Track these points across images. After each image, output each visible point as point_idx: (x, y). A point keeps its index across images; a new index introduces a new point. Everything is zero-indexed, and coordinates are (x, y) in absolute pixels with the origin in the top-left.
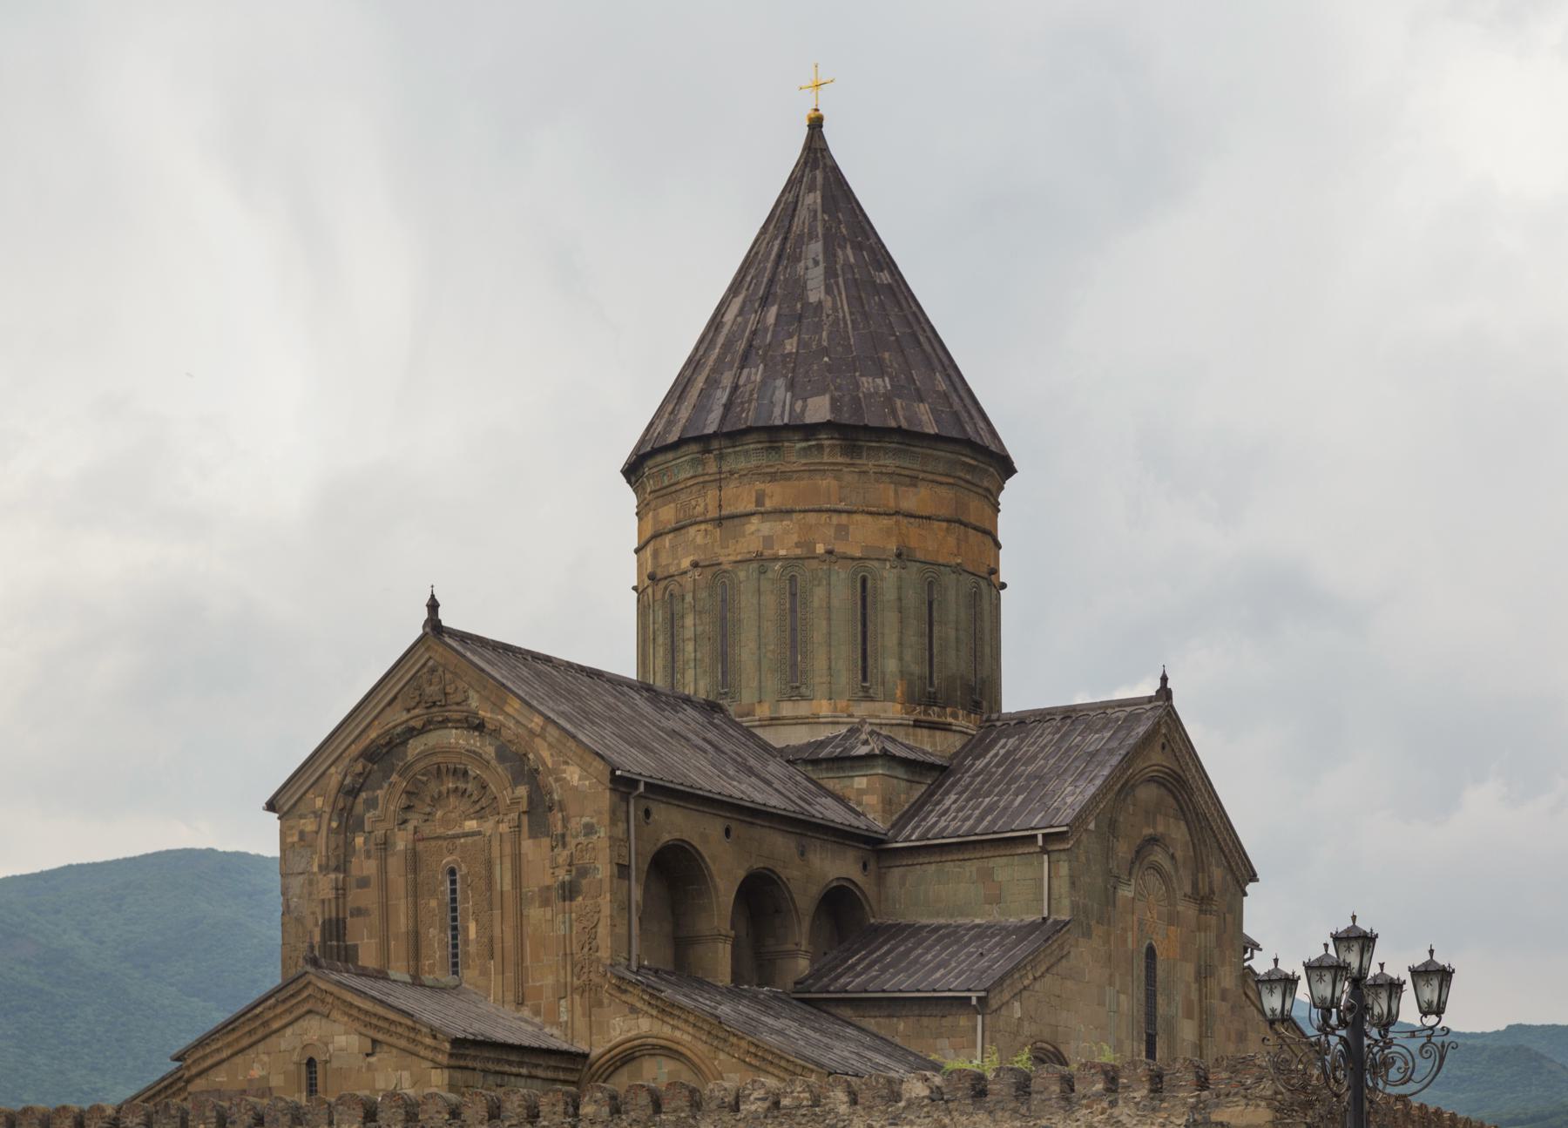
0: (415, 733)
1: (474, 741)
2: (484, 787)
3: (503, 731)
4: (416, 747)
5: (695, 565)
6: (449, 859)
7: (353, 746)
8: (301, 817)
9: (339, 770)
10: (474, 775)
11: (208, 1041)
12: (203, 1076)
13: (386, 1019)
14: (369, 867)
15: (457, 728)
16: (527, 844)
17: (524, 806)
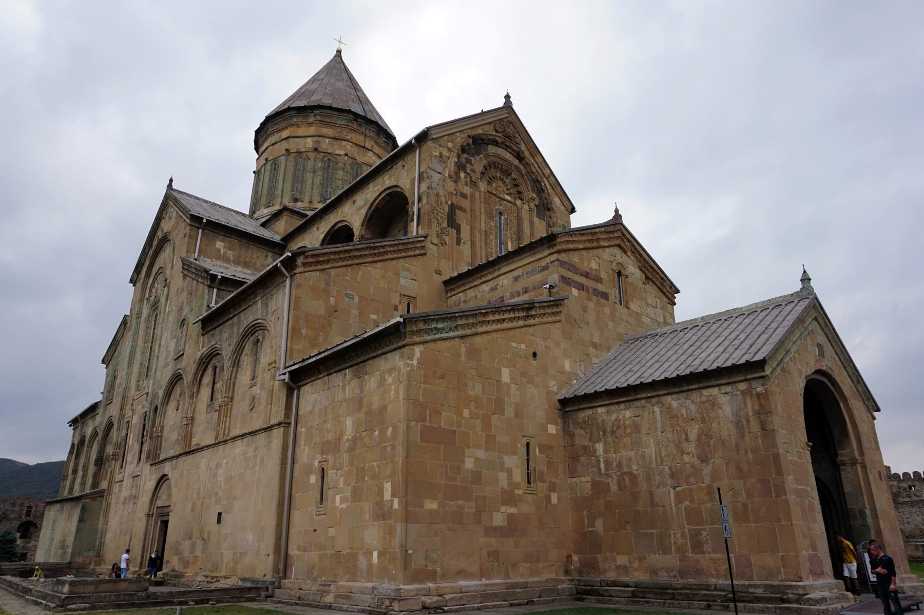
0: (494, 143)
1: (516, 162)
2: (517, 186)
3: (532, 166)
4: (492, 149)
5: (346, 155)
6: (500, 207)
7: (469, 130)
8: (440, 146)
9: (462, 136)
10: (515, 177)
11: (572, 233)
12: (567, 253)
13: (652, 268)
14: (467, 190)
15: (510, 153)
16: (536, 220)
17: (537, 204)
